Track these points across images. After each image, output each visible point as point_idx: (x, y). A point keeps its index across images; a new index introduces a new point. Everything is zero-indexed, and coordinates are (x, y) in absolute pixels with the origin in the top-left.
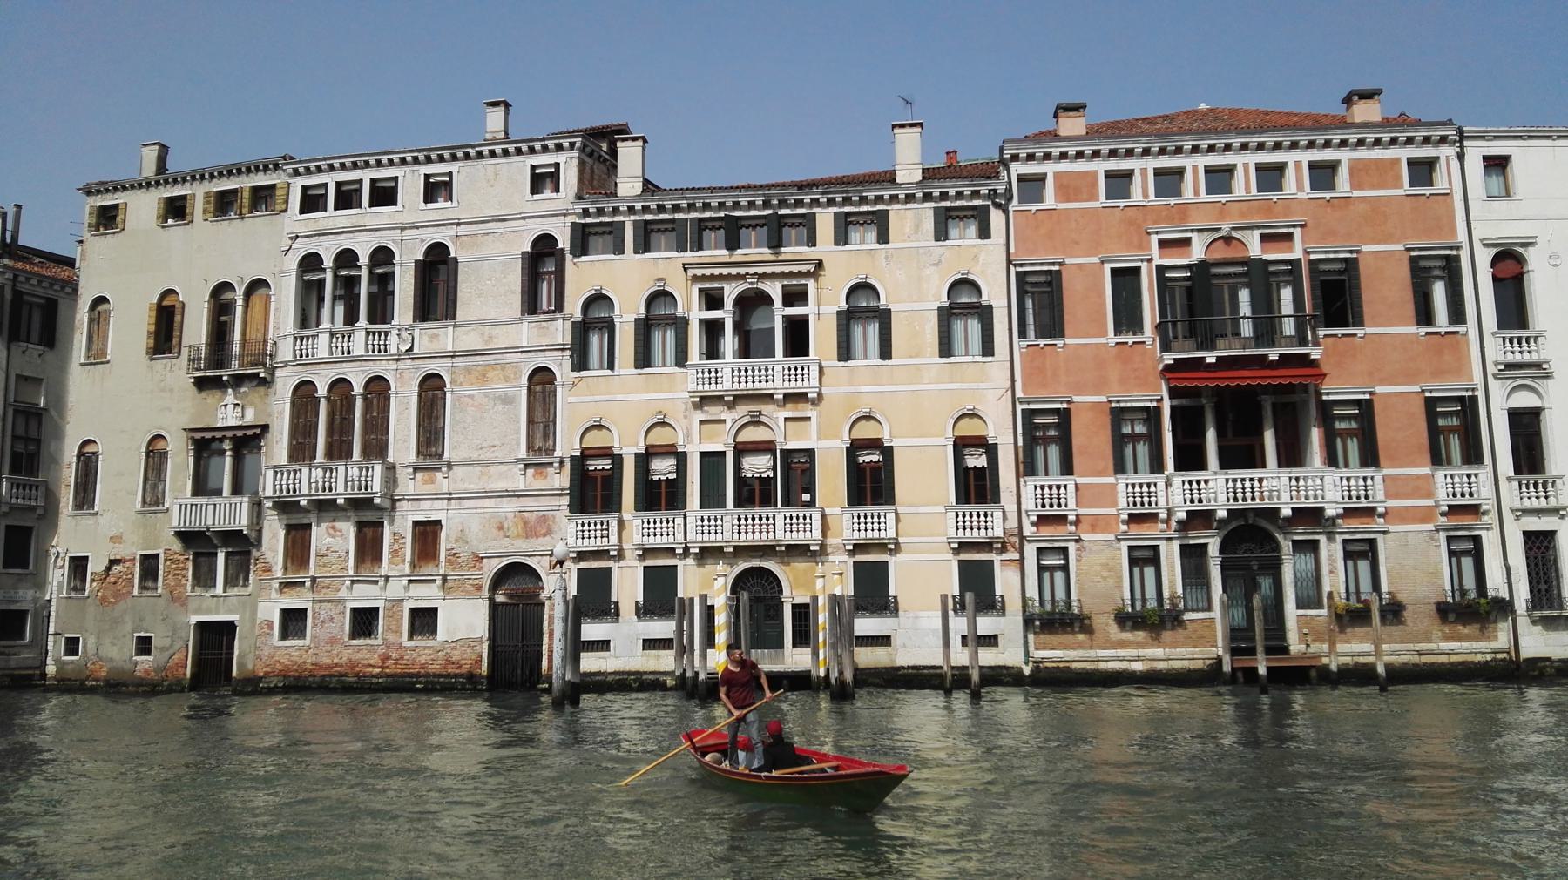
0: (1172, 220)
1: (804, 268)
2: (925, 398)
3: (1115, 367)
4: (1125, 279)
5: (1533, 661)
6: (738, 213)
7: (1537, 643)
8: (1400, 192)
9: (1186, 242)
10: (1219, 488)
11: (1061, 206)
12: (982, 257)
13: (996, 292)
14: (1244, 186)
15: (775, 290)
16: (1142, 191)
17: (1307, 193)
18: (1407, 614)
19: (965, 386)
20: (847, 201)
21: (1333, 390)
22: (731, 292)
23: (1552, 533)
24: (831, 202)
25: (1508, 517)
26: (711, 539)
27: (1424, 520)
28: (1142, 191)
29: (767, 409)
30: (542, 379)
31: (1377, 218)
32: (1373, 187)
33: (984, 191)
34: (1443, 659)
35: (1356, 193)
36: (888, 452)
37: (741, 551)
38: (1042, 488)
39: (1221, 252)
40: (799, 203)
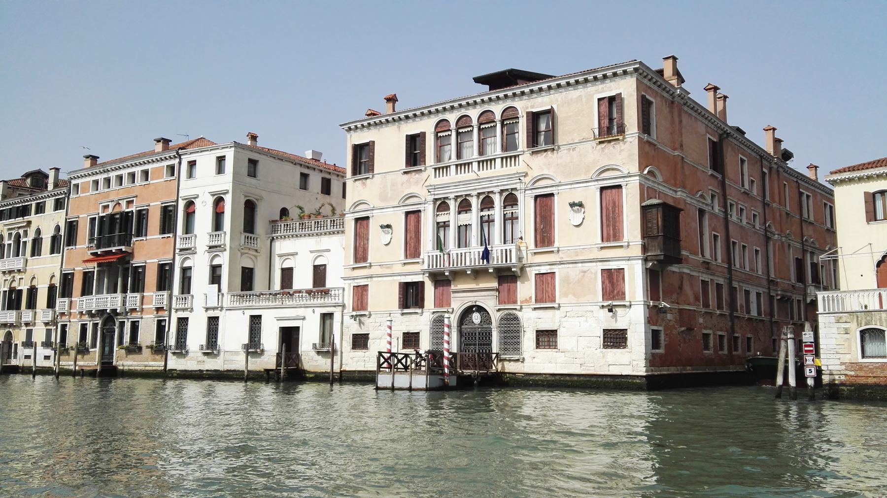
0: (105, 198)
2: (45, 269)
3: (80, 257)
4: (93, 220)
5: (171, 370)
7: (174, 363)
9: (107, 206)
15: (21, 231)
18: (144, 349)
21: (137, 262)
22: (14, 232)
25: (173, 311)
27: (152, 313)
29: (16, 275)
34: (150, 368)
39: (117, 210)
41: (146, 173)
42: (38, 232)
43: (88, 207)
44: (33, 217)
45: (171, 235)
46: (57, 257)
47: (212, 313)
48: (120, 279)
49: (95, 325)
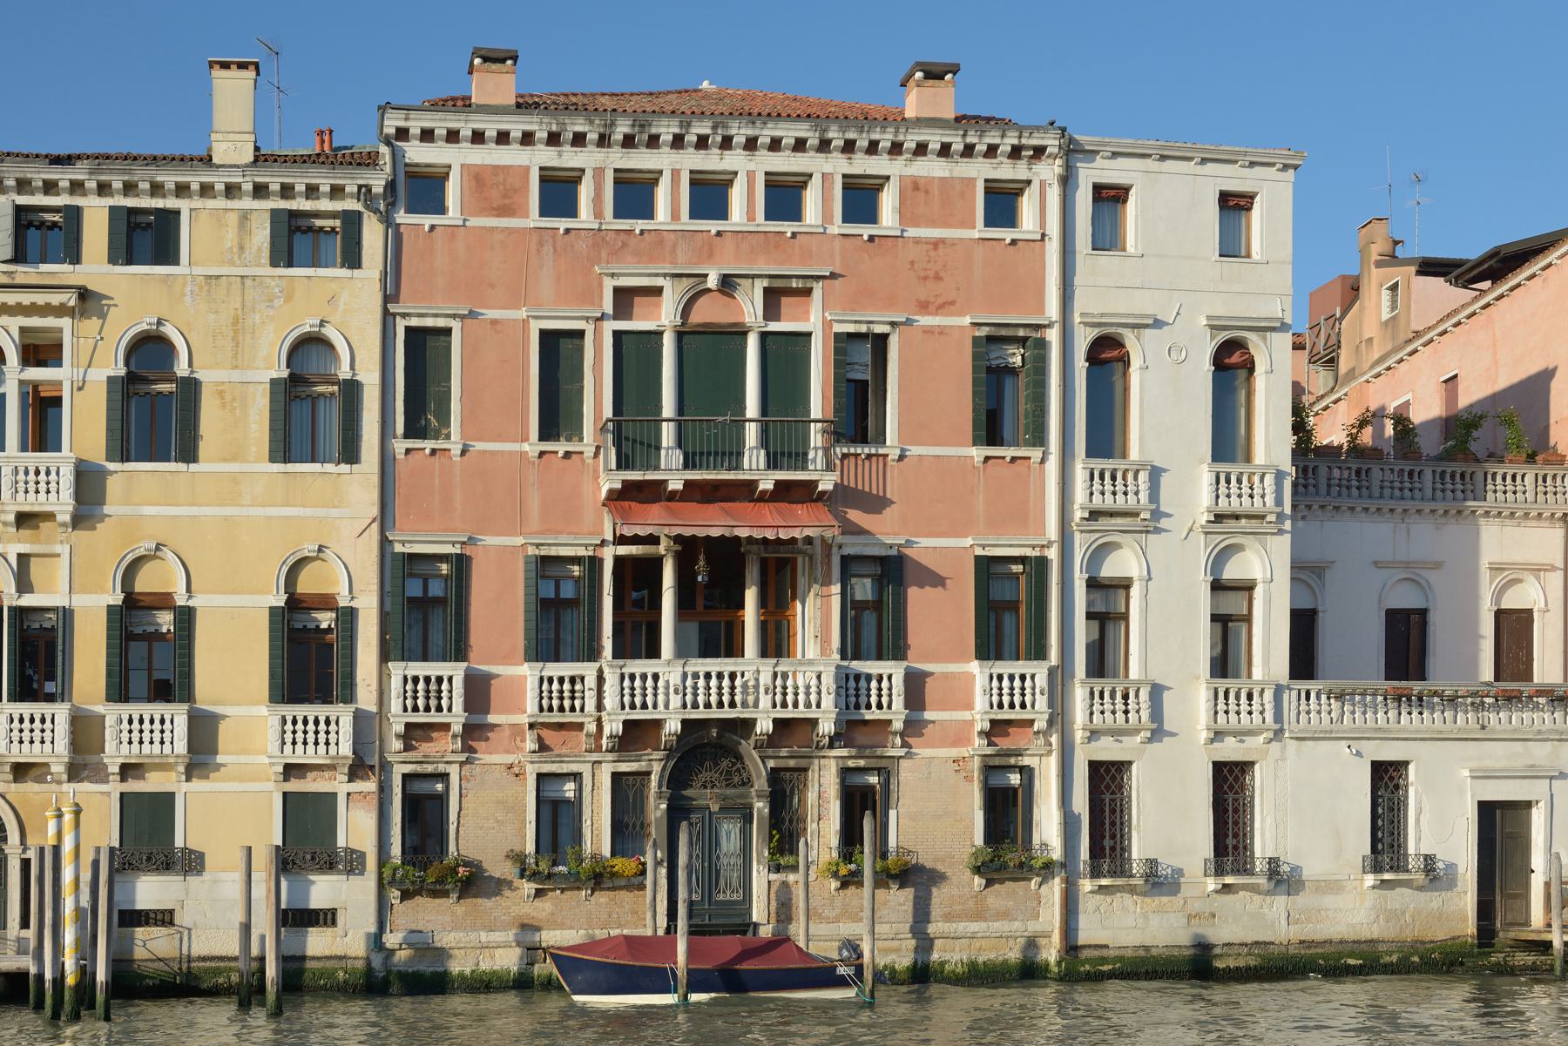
1: (55, 299)
2: (242, 530)
11: (474, 222)
12: (344, 298)
13: (361, 354)
14: (744, 205)
16: (593, 206)
17: (837, 227)
19: (309, 512)
20: (129, 188)
24: (103, 189)
28: (593, 206)
31: (933, 276)
32: (932, 223)
35: (912, 232)
36: (186, 617)
38: (416, 680)
44: (95, 265)
45: (1035, 454)
47: (1230, 750)
48: (751, 596)
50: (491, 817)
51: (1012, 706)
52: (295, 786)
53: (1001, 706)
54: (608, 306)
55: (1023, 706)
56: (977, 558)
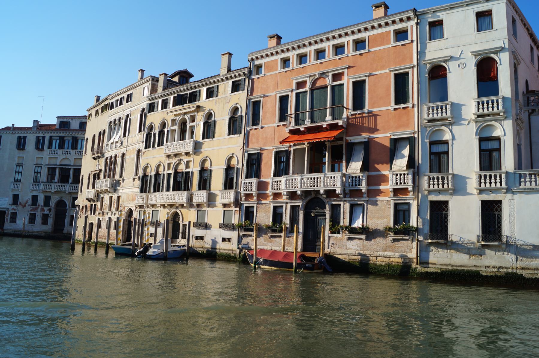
4: (284, 100)
6: (182, 94)
8: (390, 46)
9: (305, 83)
10: (301, 181)
15: (187, 117)
23: (447, 202)
24: (203, 85)
26: (163, 202)
28: (294, 63)
30: (139, 151)
33: (241, 74)
37: (171, 206)
40: (195, 87)
41: (359, 44)
42: (209, 115)
43: (274, 85)
46: (239, 139)
49: (294, 210)
50: (264, 216)
51: (401, 183)
52: (226, 209)
53: (397, 183)
54: (294, 87)
55: (405, 183)
56: (391, 139)
